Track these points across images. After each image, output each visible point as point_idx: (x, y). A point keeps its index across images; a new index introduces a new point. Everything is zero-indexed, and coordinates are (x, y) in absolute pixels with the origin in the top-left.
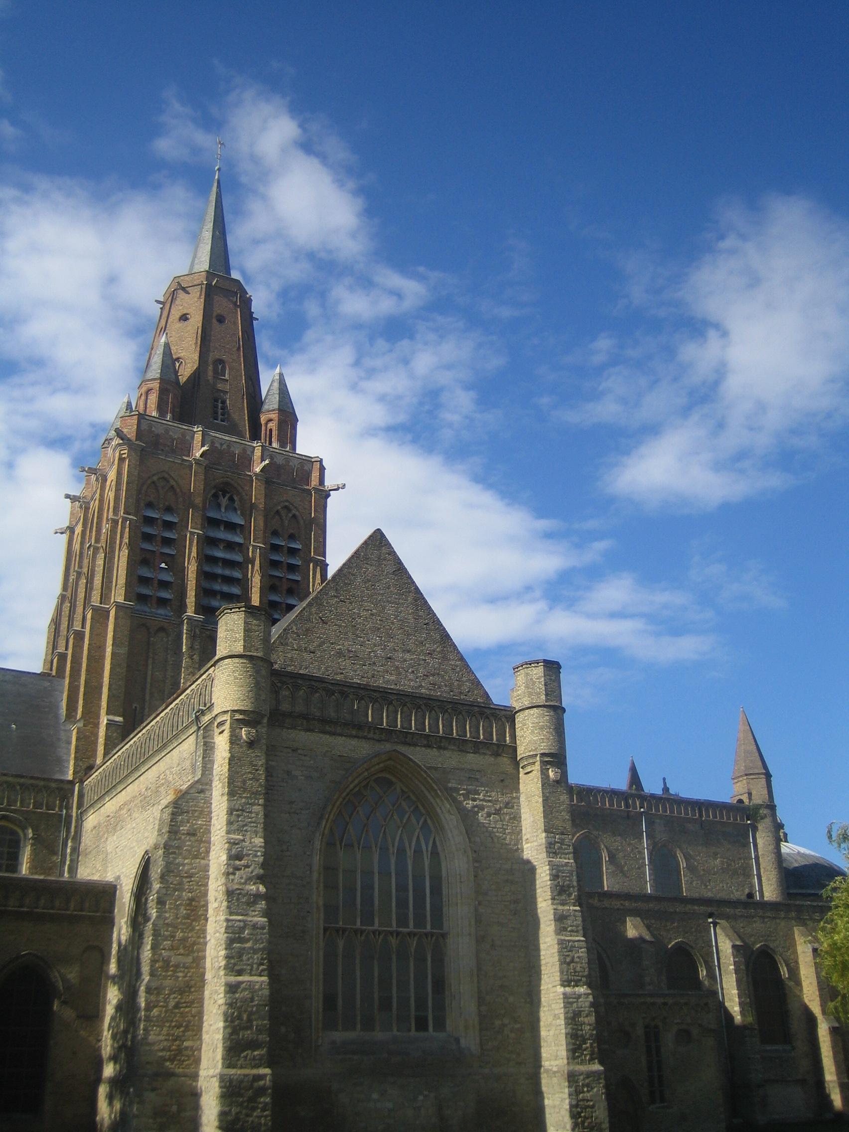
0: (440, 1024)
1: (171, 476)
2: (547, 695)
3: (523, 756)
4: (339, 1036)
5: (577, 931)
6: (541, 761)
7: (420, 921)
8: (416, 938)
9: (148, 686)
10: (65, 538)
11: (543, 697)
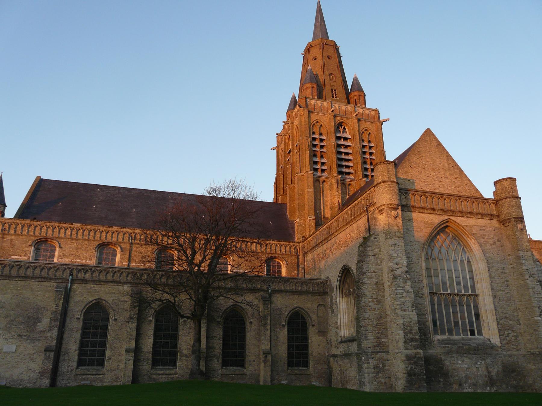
0: (480, 333)
1: (321, 121)
8: (466, 297)
10: (275, 151)
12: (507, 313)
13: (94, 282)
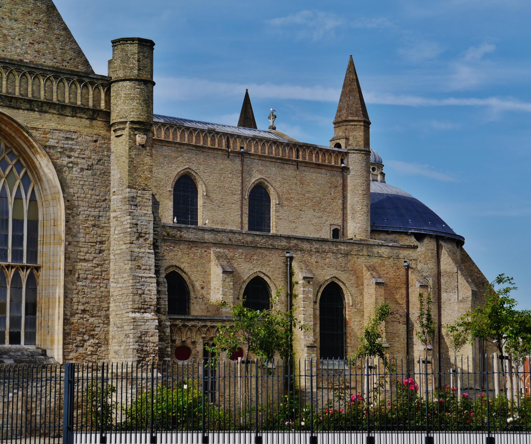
0: (31, 338)
2: (139, 70)
3: (114, 121)
5: (150, 270)
6: (131, 128)
7: (18, 255)
8: (13, 270)
11: (136, 72)
12: (88, 303)
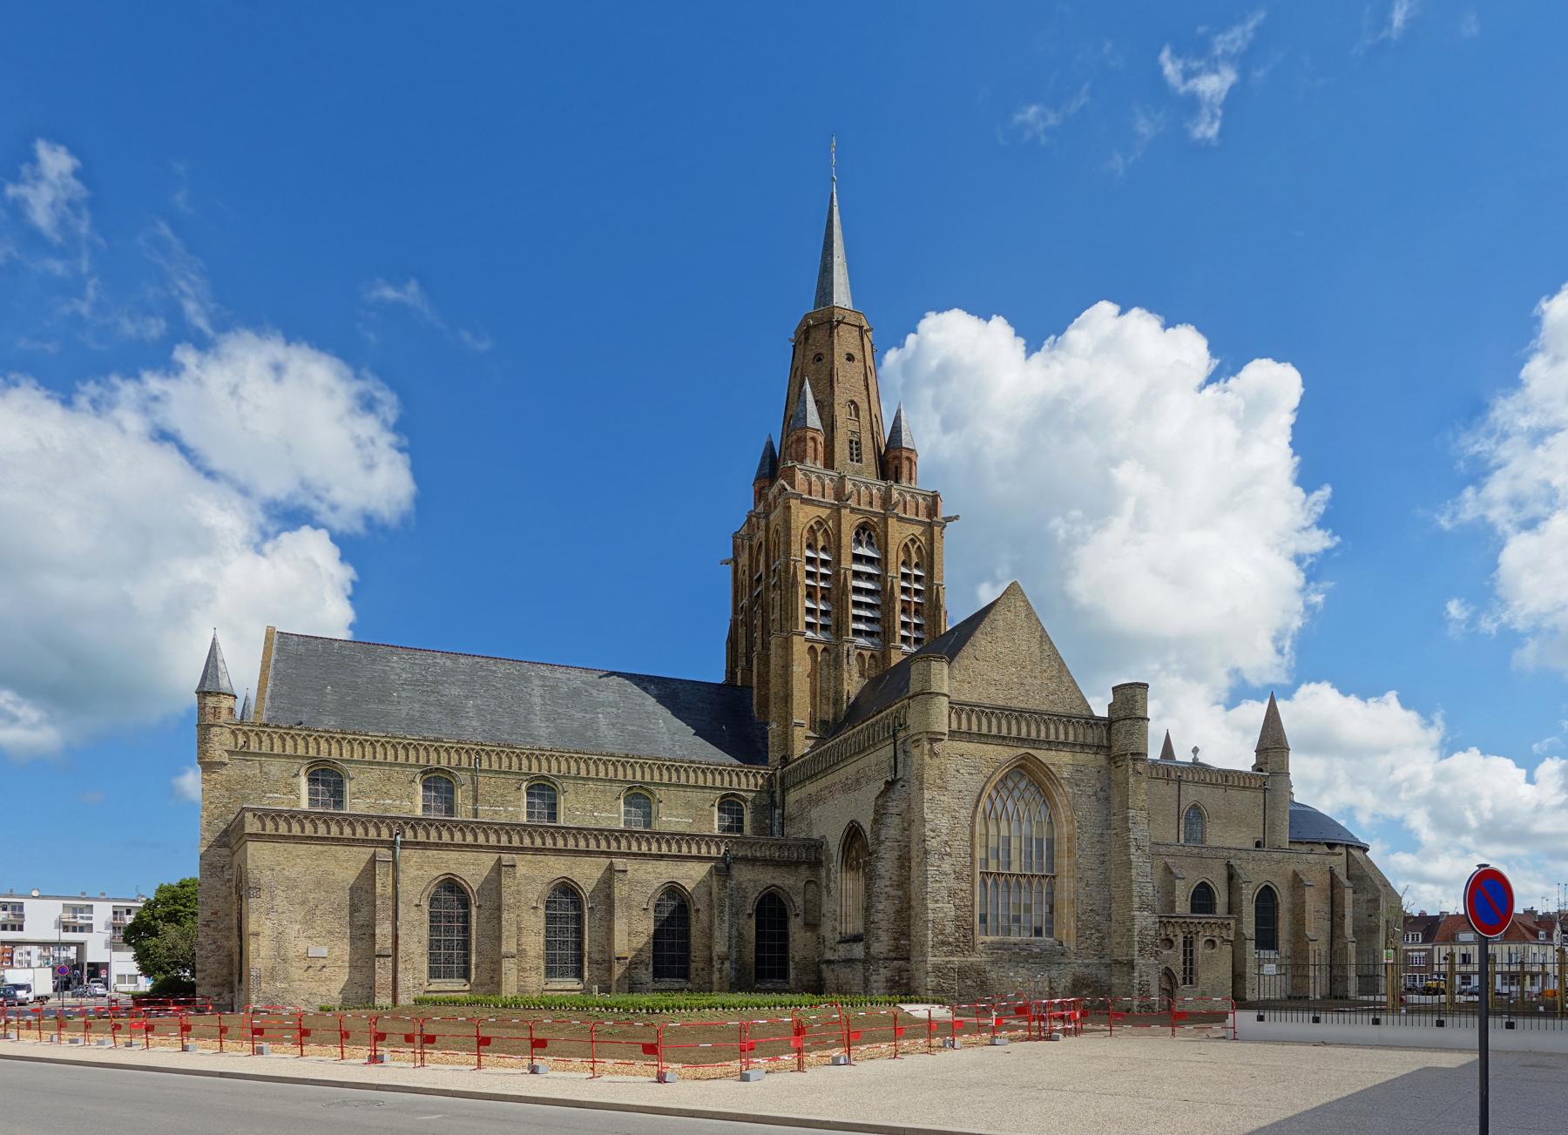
4: (988, 939)
9: (818, 694)
10: (730, 568)
13: (439, 846)
